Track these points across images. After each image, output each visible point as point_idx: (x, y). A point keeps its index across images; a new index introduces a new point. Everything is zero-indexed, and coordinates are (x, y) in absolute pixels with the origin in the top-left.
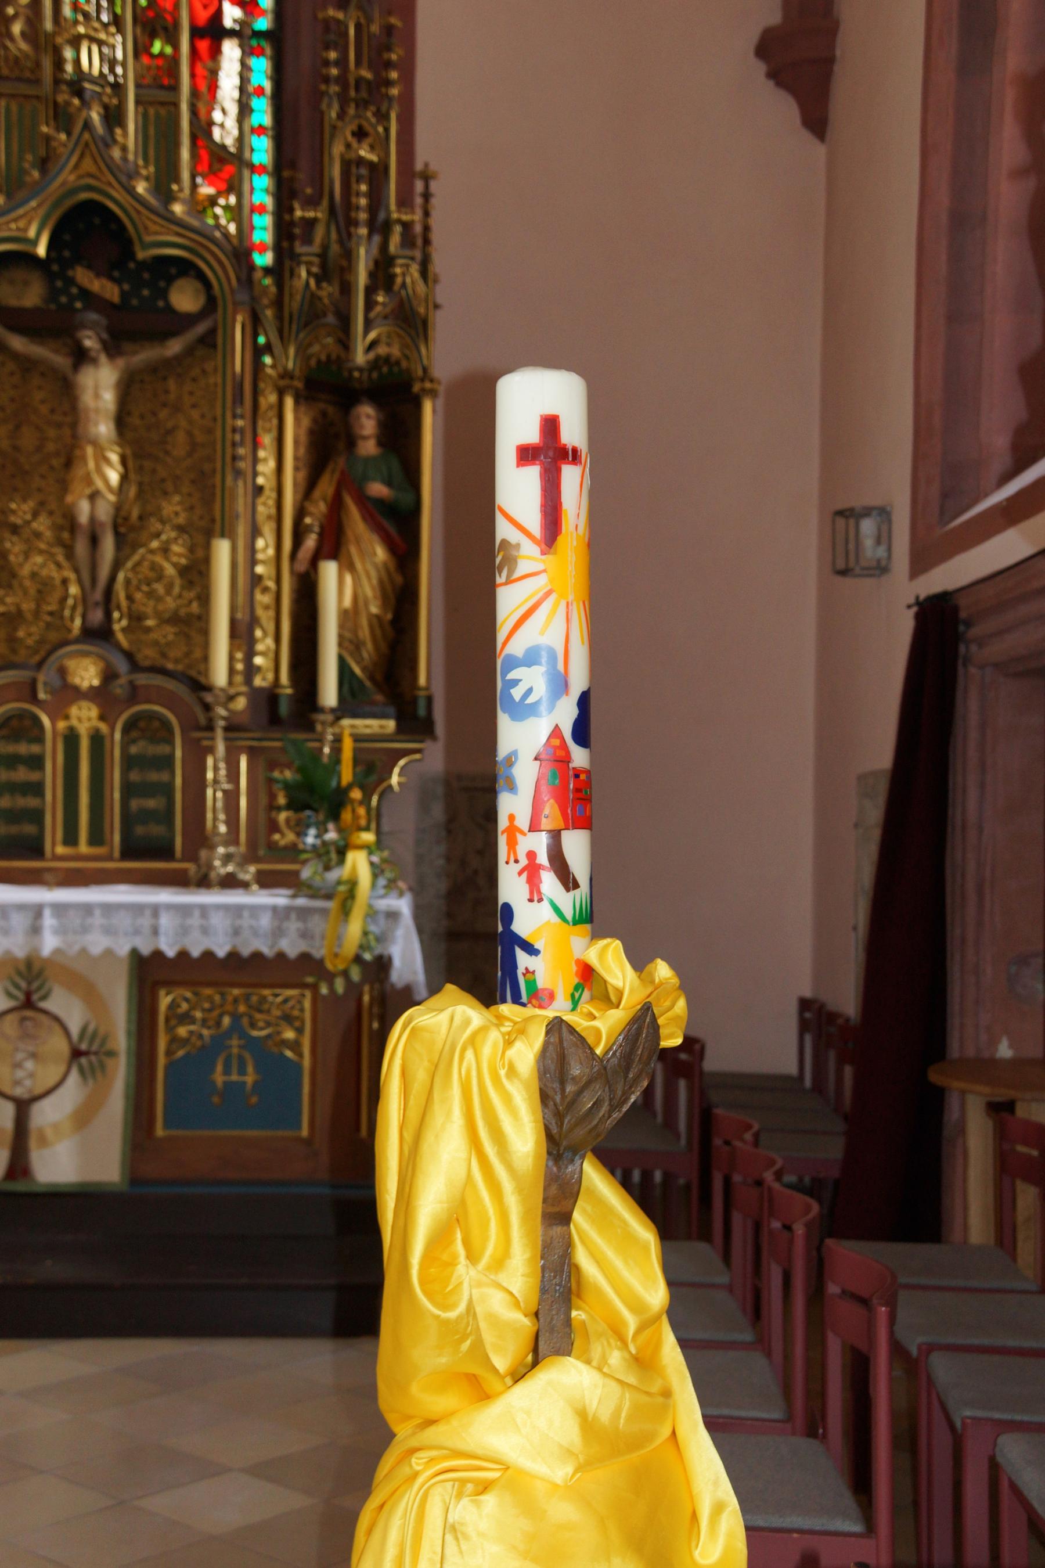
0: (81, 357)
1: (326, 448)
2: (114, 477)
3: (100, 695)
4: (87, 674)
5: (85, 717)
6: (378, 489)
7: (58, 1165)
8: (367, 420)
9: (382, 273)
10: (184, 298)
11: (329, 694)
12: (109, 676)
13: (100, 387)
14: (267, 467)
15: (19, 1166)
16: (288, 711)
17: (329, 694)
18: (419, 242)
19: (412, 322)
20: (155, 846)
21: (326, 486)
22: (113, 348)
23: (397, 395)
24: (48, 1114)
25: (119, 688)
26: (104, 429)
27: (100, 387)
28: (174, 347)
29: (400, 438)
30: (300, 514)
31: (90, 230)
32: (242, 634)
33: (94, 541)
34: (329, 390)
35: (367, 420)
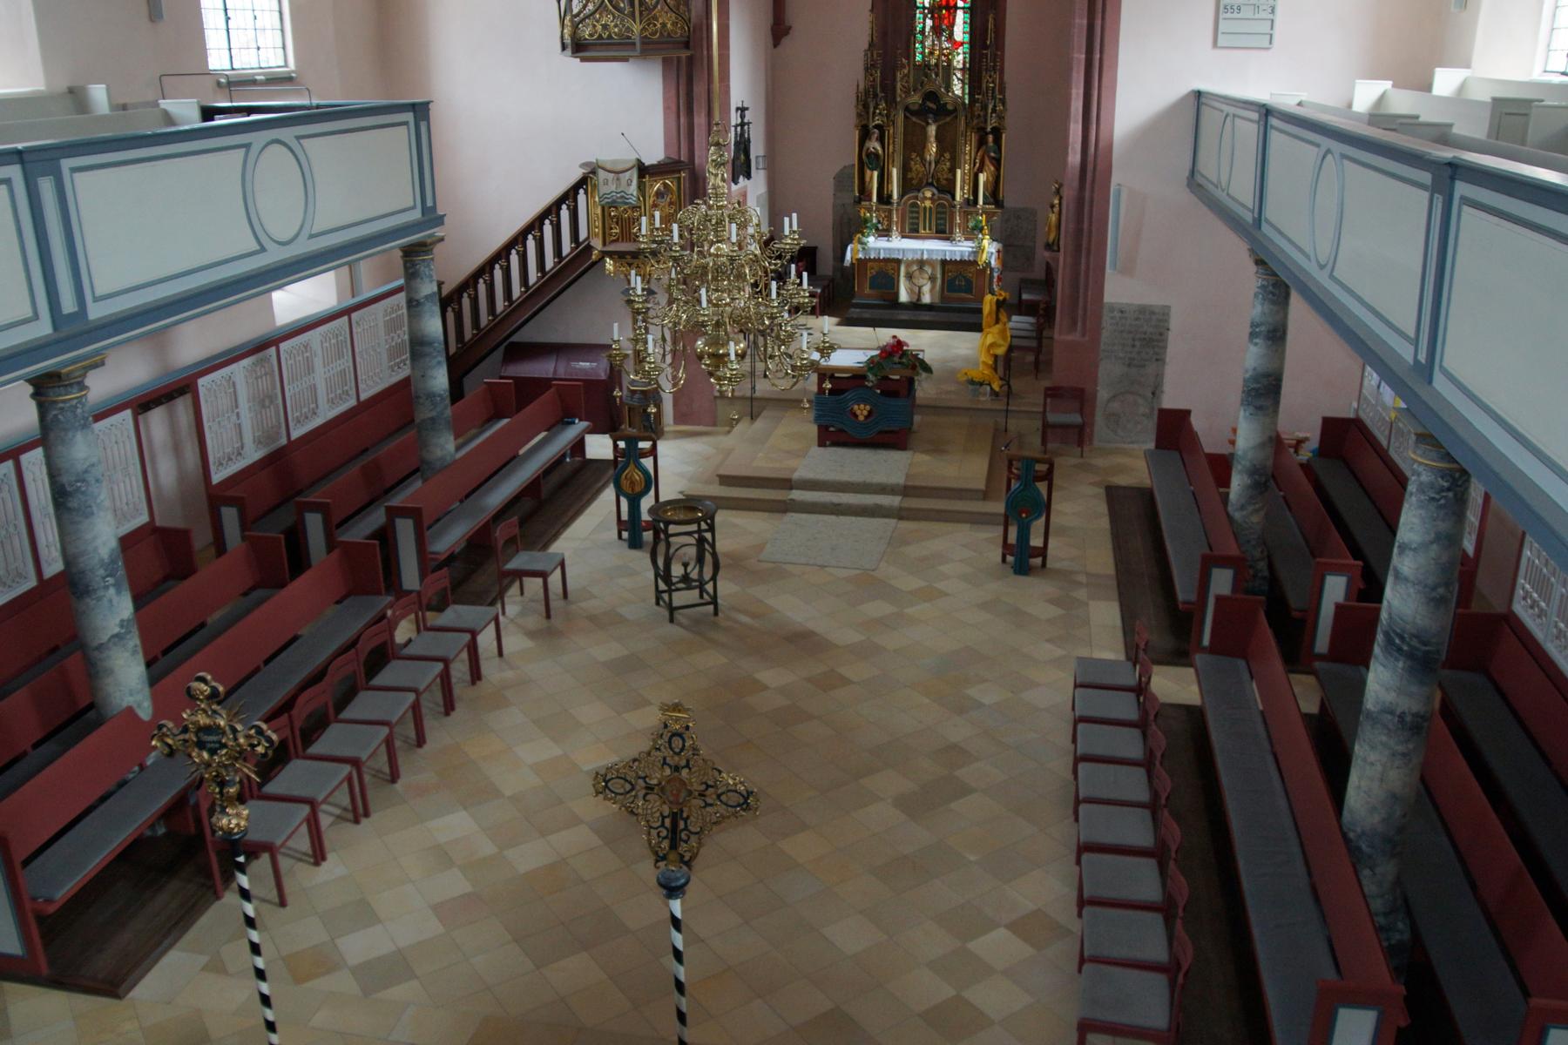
1: (982, 142)
4: (929, 194)
5: (928, 204)
7: (926, 299)
9: (994, 110)
11: (981, 201)
13: (932, 130)
15: (919, 299)
17: (981, 201)
18: (1003, 102)
19: (1001, 118)
20: (943, 233)
23: (997, 132)
24: (926, 289)
27: (932, 130)
29: (997, 141)
31: (932, 96)
32: (962, 189)
35: (990, 138)
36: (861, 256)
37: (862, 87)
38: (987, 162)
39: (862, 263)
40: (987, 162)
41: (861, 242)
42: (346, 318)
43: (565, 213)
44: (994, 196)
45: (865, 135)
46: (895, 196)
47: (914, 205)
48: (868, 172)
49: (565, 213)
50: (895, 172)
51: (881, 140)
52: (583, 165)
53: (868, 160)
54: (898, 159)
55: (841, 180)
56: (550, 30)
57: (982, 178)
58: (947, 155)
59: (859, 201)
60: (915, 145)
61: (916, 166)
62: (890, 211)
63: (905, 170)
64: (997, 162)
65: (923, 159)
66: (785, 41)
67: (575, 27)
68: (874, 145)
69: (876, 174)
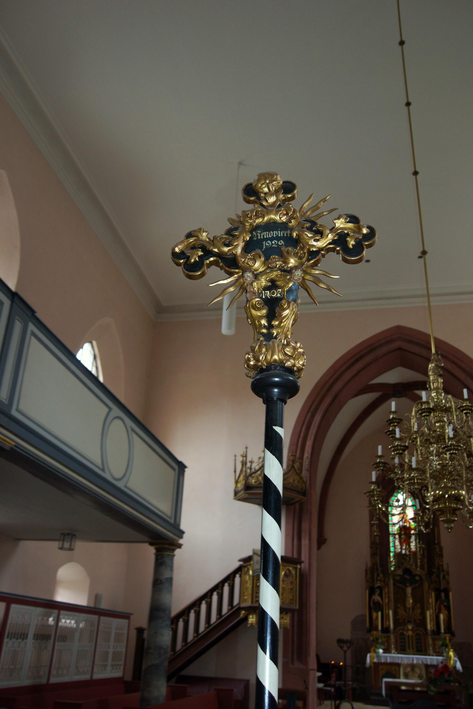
0: (406, 586)
1: (438, 598)
2: (411, 601)
3: (412, 630)
4: (410, 627)
5: (410, 633)
6: (445, 604)
8: (443, 595)
9: (444, 577)
10: (417, 578)
12: (413, 628)
13: (409, 590)
14: (431, 600)
16: (437, 631)
18: (448, 573)
19: (448, 583)
21: (438, 603)
22: (410, 586)
23: (446, 591)
25: (415, 629)
26: (409, 595)
27: (409, 590)
28: (417, 585)
29: (447, 596)
30: (435, 606)
33: (409, 609)
34: (438, 591)
35: (443, 595)
36: (375, 660)
37: (369, 565)
38: (442, 607)
39: (377, 665)
40: (442, 607)
41: (375, 652)
42: (96, 617)
43: (226, 589)
44: (449, 629)
45: (372, 591)
46: (392, 626)
47: (402, 634)
48: (374, 615)
49: (226, 589)
50: (391, 612)
51: (381, 595)
52: (240, 560)
53: (375, 607)
54: (392, 604)
55: (357, 623)
56: (229, 485)
57: (442, 616)
58: (418, 605)
59: (369, 631)
60: (400, 599)
61: (401, 611)
62: (388, 638)
63: (395, 614)
64: (448, 608)
65: (405, 607)
66: (324, 547)
67: (247, 478)
68: (377, 598)
69: (380, 613)
